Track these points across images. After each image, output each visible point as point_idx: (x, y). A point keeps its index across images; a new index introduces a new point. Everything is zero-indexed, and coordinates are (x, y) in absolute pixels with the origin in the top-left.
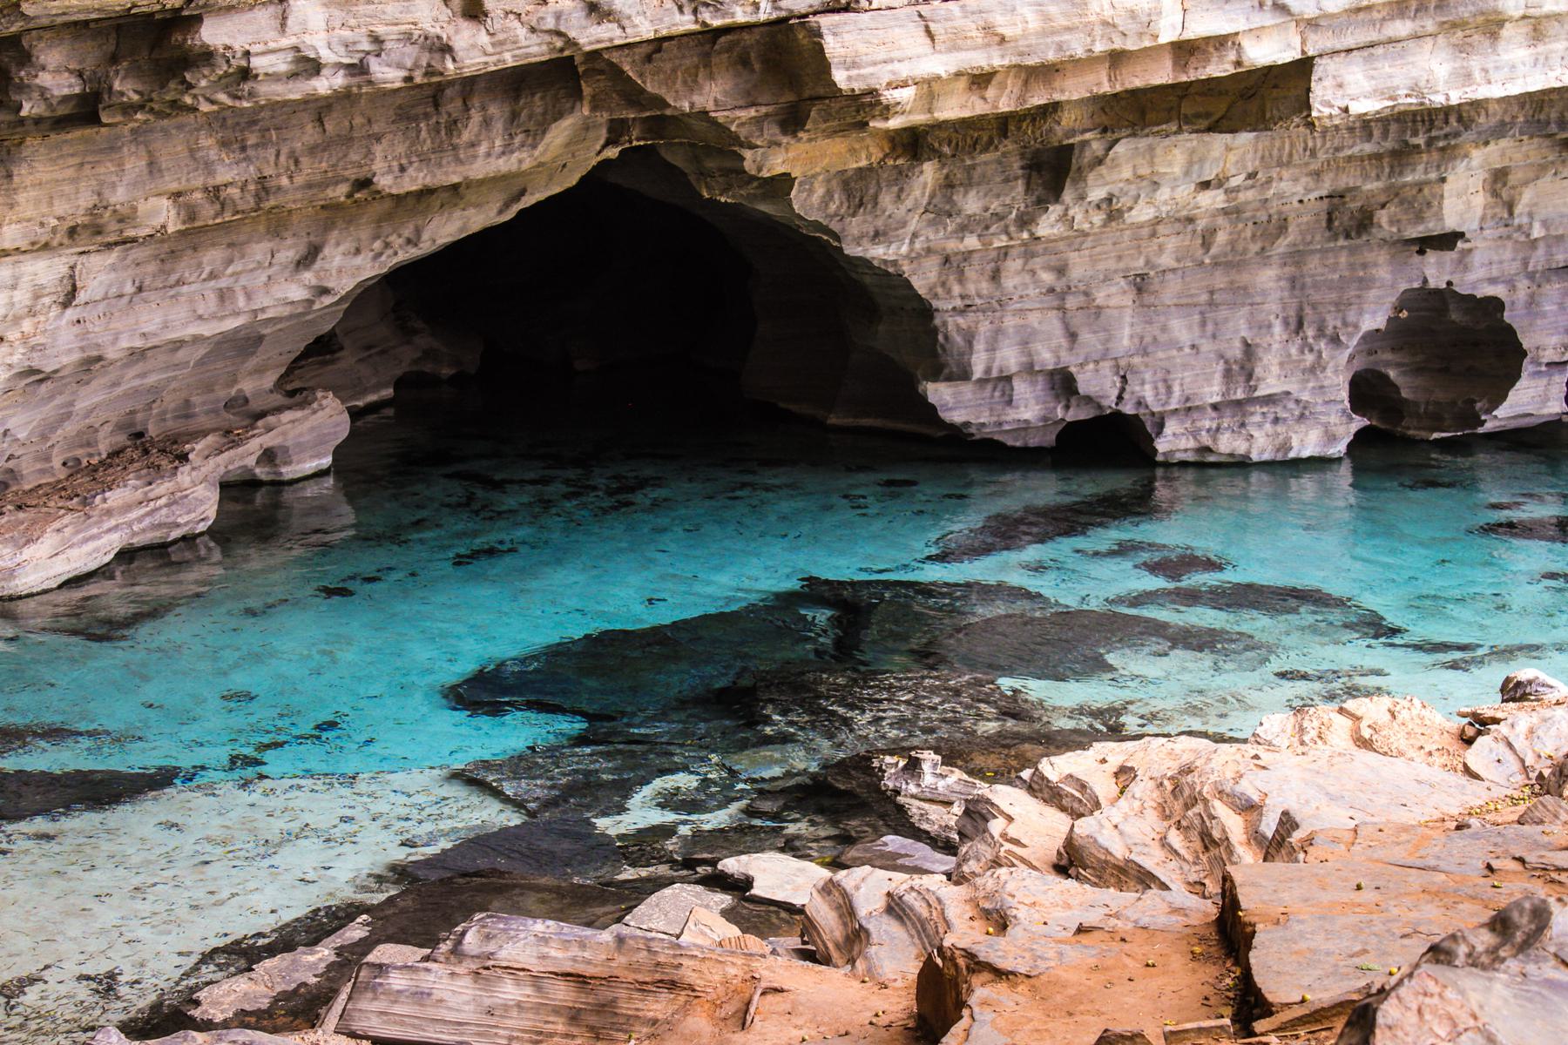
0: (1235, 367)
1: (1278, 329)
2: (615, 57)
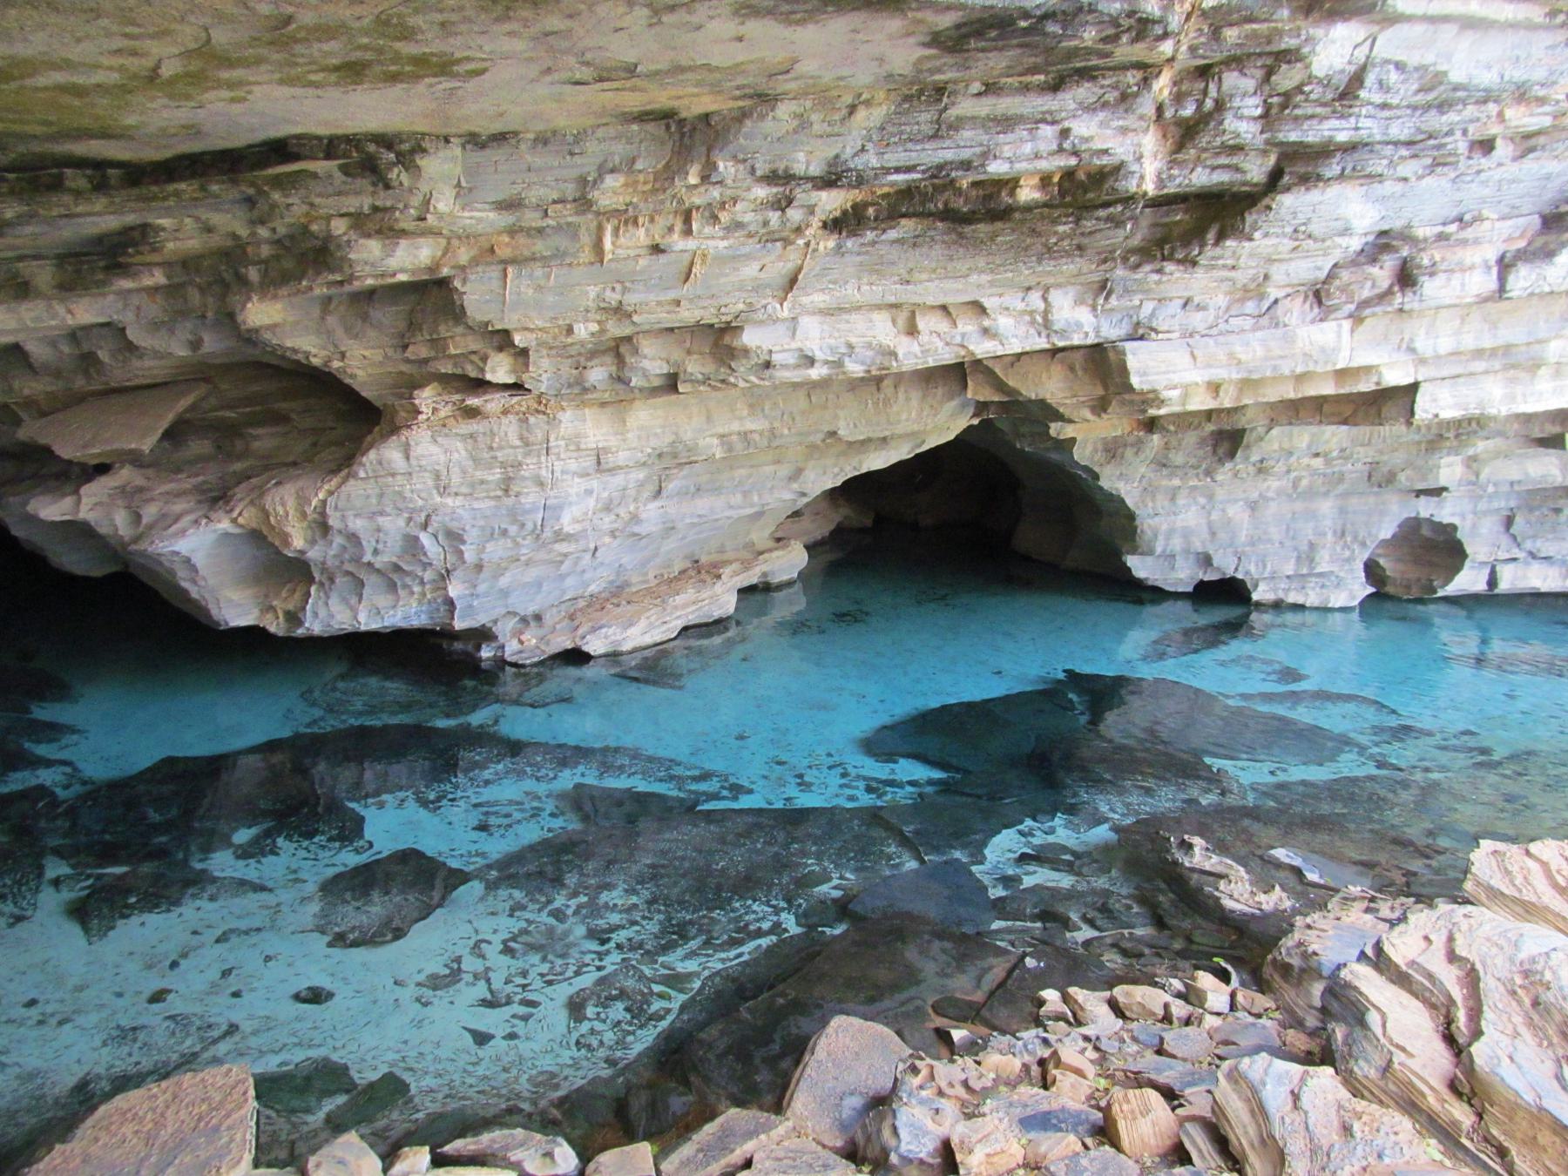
1: (1330, 536)
2: (990, 364)
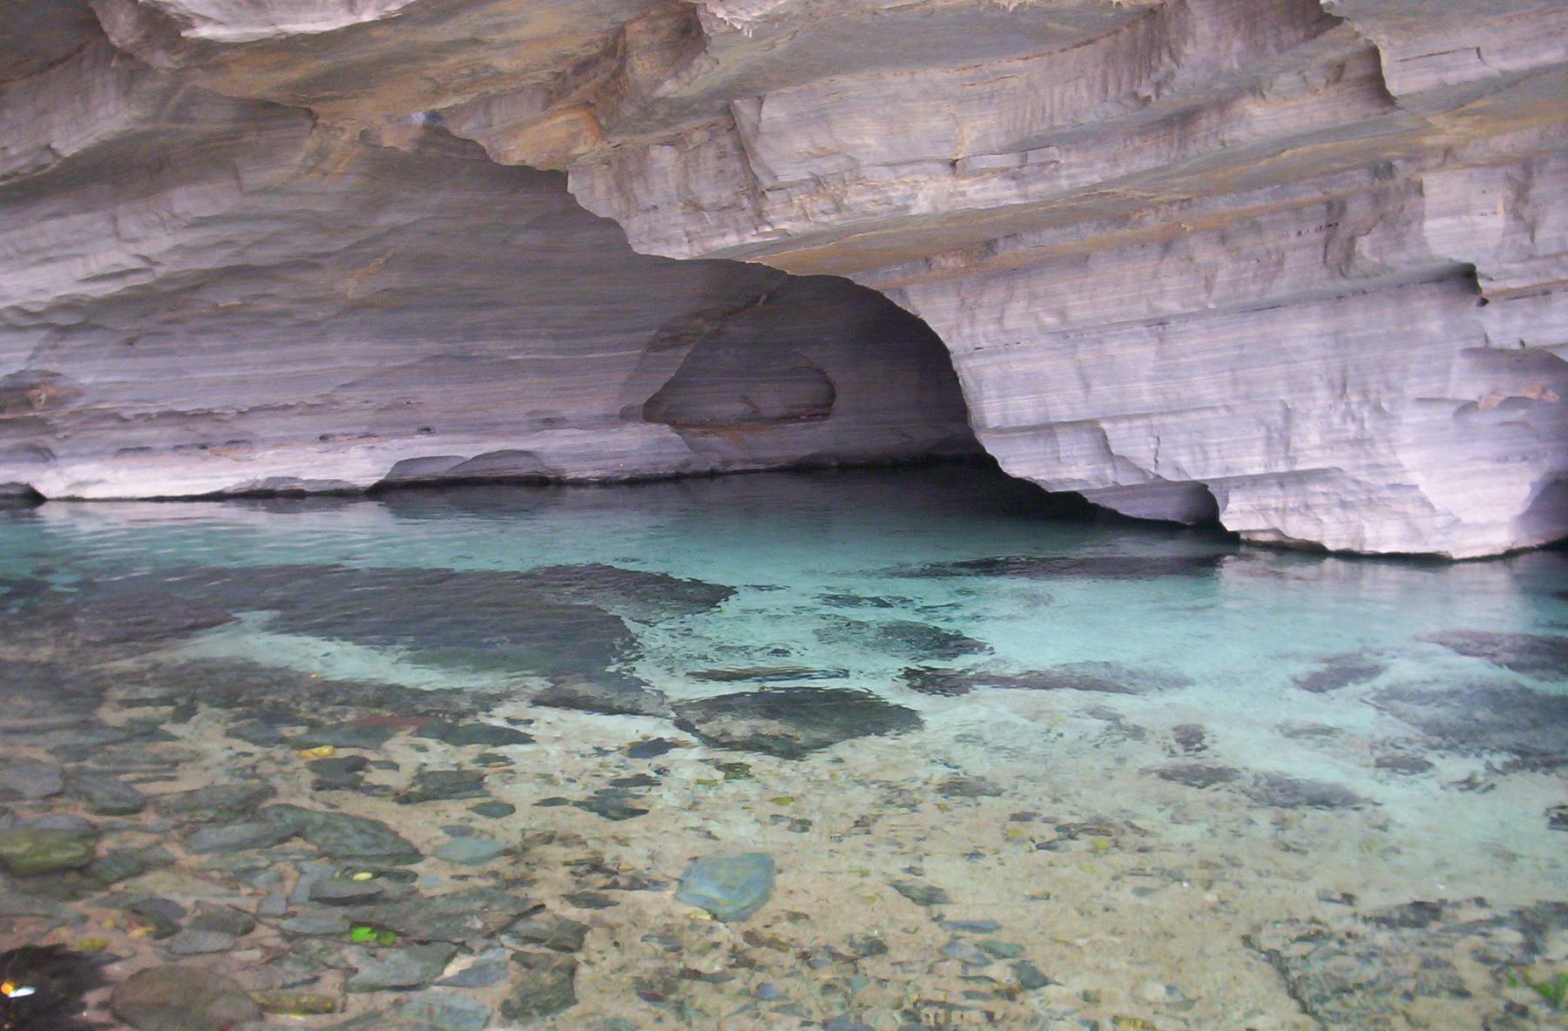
0: (1275, 435)
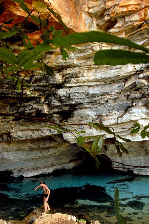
1: (143, 163)
